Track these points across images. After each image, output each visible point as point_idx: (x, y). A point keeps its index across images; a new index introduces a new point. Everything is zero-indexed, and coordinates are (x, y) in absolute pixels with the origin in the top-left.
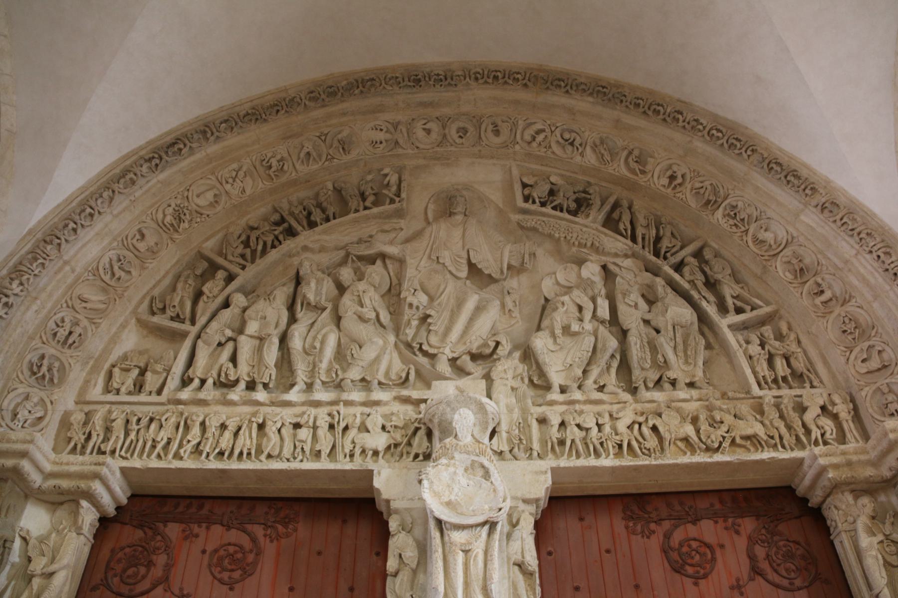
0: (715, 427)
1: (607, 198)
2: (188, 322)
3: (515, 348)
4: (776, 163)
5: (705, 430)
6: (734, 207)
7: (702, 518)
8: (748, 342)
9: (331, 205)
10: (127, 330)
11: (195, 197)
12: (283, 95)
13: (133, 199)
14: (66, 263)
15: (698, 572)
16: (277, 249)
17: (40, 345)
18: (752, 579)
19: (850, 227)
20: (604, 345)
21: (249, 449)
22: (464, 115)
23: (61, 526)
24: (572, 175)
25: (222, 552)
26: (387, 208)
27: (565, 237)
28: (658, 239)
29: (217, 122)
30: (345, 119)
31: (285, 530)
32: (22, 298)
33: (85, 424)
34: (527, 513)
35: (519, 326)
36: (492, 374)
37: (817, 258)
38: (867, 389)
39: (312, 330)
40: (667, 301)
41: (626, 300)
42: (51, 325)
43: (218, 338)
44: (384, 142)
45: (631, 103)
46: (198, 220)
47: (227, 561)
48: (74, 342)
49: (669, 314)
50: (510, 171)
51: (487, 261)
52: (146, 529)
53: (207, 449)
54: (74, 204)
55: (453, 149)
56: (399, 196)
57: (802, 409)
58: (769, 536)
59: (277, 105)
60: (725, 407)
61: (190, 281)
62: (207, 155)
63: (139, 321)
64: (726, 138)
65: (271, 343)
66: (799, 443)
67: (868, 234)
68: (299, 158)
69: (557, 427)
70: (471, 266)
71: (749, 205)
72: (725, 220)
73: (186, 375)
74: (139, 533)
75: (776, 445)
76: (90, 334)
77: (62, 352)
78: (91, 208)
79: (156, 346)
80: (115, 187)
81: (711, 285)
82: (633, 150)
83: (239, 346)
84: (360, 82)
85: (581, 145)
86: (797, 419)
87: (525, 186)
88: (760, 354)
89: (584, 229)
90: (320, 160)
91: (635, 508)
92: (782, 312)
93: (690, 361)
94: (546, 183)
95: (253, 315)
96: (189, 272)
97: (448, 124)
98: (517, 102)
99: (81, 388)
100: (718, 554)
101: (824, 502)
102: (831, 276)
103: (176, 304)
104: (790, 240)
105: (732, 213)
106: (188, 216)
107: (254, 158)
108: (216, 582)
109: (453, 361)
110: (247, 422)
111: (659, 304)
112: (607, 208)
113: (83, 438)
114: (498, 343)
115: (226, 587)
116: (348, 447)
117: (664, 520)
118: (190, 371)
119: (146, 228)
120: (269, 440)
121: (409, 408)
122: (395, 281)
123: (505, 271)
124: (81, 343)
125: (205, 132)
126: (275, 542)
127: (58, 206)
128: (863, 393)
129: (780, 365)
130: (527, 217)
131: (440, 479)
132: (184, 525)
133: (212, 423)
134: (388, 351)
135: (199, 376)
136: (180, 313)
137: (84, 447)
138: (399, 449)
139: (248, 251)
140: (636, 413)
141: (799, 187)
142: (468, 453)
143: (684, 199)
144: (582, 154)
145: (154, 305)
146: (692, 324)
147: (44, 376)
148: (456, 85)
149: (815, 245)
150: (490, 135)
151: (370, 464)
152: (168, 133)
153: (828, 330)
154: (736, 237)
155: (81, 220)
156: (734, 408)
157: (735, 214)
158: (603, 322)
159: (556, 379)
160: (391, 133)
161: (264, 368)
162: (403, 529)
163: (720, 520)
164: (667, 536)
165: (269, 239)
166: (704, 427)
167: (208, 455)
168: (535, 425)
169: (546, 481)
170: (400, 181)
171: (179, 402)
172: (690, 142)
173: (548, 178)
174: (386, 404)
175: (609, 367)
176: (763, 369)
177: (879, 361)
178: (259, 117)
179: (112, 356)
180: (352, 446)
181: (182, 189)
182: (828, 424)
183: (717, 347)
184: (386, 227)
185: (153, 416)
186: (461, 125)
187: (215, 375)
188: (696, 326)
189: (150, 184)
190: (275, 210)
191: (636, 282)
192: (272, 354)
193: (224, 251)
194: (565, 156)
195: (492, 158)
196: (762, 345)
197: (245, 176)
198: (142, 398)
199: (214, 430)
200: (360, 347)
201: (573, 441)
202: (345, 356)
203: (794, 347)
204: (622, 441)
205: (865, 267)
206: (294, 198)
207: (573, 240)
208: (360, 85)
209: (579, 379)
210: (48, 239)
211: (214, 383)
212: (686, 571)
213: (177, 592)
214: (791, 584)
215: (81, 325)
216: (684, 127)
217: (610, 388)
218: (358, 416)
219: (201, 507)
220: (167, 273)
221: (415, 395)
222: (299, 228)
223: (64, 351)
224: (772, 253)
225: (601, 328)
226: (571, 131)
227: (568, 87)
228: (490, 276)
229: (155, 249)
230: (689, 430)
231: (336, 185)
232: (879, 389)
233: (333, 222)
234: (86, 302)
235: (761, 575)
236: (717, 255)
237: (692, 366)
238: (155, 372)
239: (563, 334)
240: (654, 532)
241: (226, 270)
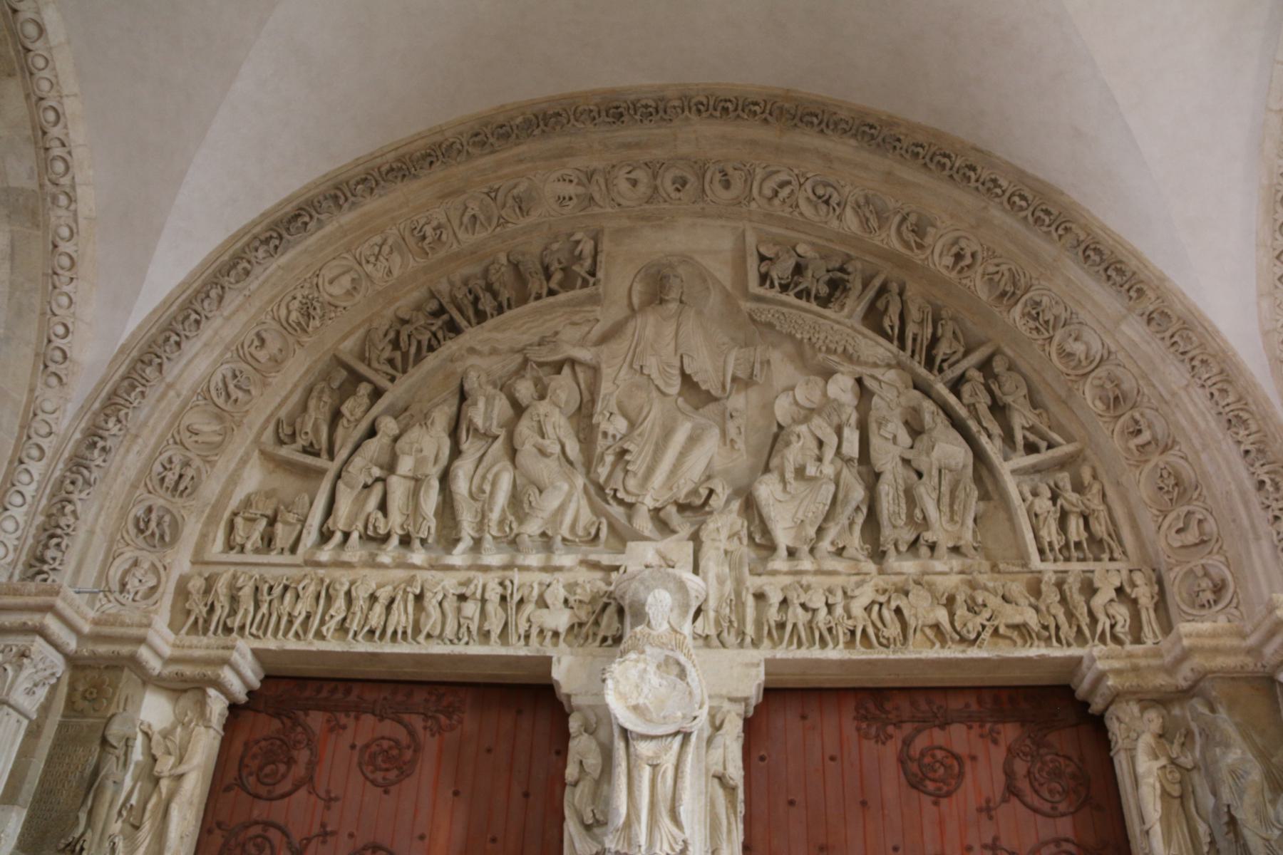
0: (975, 613)
1: (872, 277)
2: (325, 455)
3: (737, 493)
4: (1095, 249)
5: (962, 616)
6: (1038, 304)
7: (952, 722)
8: (1035, 494)
9: (505, 287)
10: (249, 466)
11: (326, 284)
12: (438, 138)
13: (247, 293)
14: (170, 386)
15: (940, 789)
16: (435, 353)
17: (146, 495)
18: (1005, 800)
19: (1181, 350)
20: (846, 496)
21: (405, 627)
22: (681, 159)
23: (187, 719)
24: (825, 243)
25: (374, 748)
26: (578, 293)
27: (810, 339)
28: (935, 340)
29: (352, 182)
30: (522, 167)
31: (448, 722)
32: (121, 438)
33: (207, 591)
34: (733, 714)
35: (742, 459)
36: (701, 534)
37: (1138, 384)
38: (1177, 569)
39: (481, 467)
40: (935, 434)
41: (882, 432)
42: (157, 468)
43: (363, 479)
44: (574, 197)
45: (907, 151)
46: (333, 315)
47: (380, 759)
48: (186, 488)
49: (935, 454)
50: (744, 237)
51: (704, 369)
52: (286, 720)
53: (354, 627)
54: (174, 308)
55: (666, 206)
57: (1090, 589)
58: (1034, 748)
59: (430, 155)
60: (990, 585)
61: (326, 398)
62: (341, 226)
63: (263, 453)
64: (1031, 209)
65: (429, 486)
66: (1080, 637)
67: (1203, 362)
68: (461, 224)
69: (777, 605)
70: (686, 378)
71: (1057, 303)
72: (1023, 322)
73: (325, 526)
74: (276, 724)
75: (1050, 638)
76: (204, 476)
77: (172, 502)
78: (197, 312)
79: (287, 485)
80: (225, 281)
81: (999, 409)
82: (908, 214)
83: (390, 490)
84: (540, 118)
85: (838, 204)
86: (1083, 603)
87: (762, 258)
88: (1049, 512)
89: (836, 327)
90: (490, 225)
91: (871, 705)
92: (1088, 452)
93: (956, 518)
94: (790, 257)
95: (407, 448)
96: (323, 384)
97: (661, 171)
98: (753, 143)
99: (197, 544)
100: (968, 766)
101: (1106, 708)
102: (1153, 412)
103: (309, 430)
104: (1106, 355)
105: (1034, 312)
106: (318, 310)
107: (402, 227)
108: (368, 784)
109: (656, 512)
110: (401, 593)
111: (925, 437)
112: (870, 294)
113: (205, 610)
114: (711, 492)
115: (380, 790)
116: (523, 627)
117: (905, 722)
118: (330, 521)
119: (266, 331)
120: (428, 616)
121: (598, 575)
122: (586, 396)
123: (728, 386)
124: (195, 489)
125: (336, 197)
126: (437, 736)
127: (155, 311)
128: (1172, 575)
129: (1075, 528)
130: (764, 306)
131: (627, 678)
132: (329, 714)
133: (359, 593)
134: (575, 498)
135: (341, 527)
136: (314, 442)
137: (207, 622)
138: (584, 630)
139: (398, 355)
140: (877, 591)
141: (1121, 286)
142: (662, 646)
143: (973, 288)
144: (839, 218)
145: (280, 430)
146: (965, 466)
147: (153, 534)
148: (671, 120)
149: (1138, 366)
150: (718, 187)
151: (549, 650)
152: (288, 200)
153: (1141, 485)
154: (1036, 346)
155: (184, 330)
156: (1003, 586)
157: (1038, 314)
158: (848, 461)
159: (783, 538)
160: (584, 185)
161: (421, 519)
162: (586, 731)
163: (976, 725)
164: (907, 743)
165: (425, 337)
166: (961, 611)
167: (356, 634)
168: (750, 601)
169: (757, 676)
170: (596, 253)
171: (319, 564)
172: (985, 208)
173: (794, 249)
174: (570, 569)
175: (851, 524)
176: (1050, 532)
177: (1197, 533)
178: (407, 173)
179: (232, 502)
180: (527, 625)
181: (309, 275)
182: (1122, 613)
183: (996, 497)
184: (576, 318)
185: (288, 583)
186: (678, 173)
187: (361, 527)
188: (970, 470)
189: (268, 272)
190: (432, 295)
191: (899, 404)
192: (431, 500)
193: (367, 355)
194: (817, 219)
195: (720, 217)
196: (1054, 499)
197: (391, 252)
198: (273, 557)
199: (361, 602)
200: (541, 492)
201: (795, 625)
202: (521, 502)
203: (1096, 503)
204: (855, 627)
205: (1195, 405)
206: (457, 278)
207: (820, 342)
208: (541, 123)
209: (811, 540)
210: (146, 358)
211: (360, 537)
212: (925, 786)
213: (322, 794)
214: (1053, 808)
215: (194, 466)
216: (977, 189)
217: (850, 552)
218: (536, 586)
219: (348, 692)
220: (295, 386)
221: (606, 559)
223: (174, 500)
224: (1081, 372)
225: (845, 472)
226: (826, 185)
227: (823, 126)
228: (708, 392)
229: (279, 357)
230: (942, 615)
231: (511, 258)
232: (1191, 571)
233: (508, 314)
234: (197, 434)
235: (1017, 795)
236: (1011, 367)
237: (958, 526)
238: (286, 523)
239: (796, 478)
240: (891, 737)
241: (369, 381)
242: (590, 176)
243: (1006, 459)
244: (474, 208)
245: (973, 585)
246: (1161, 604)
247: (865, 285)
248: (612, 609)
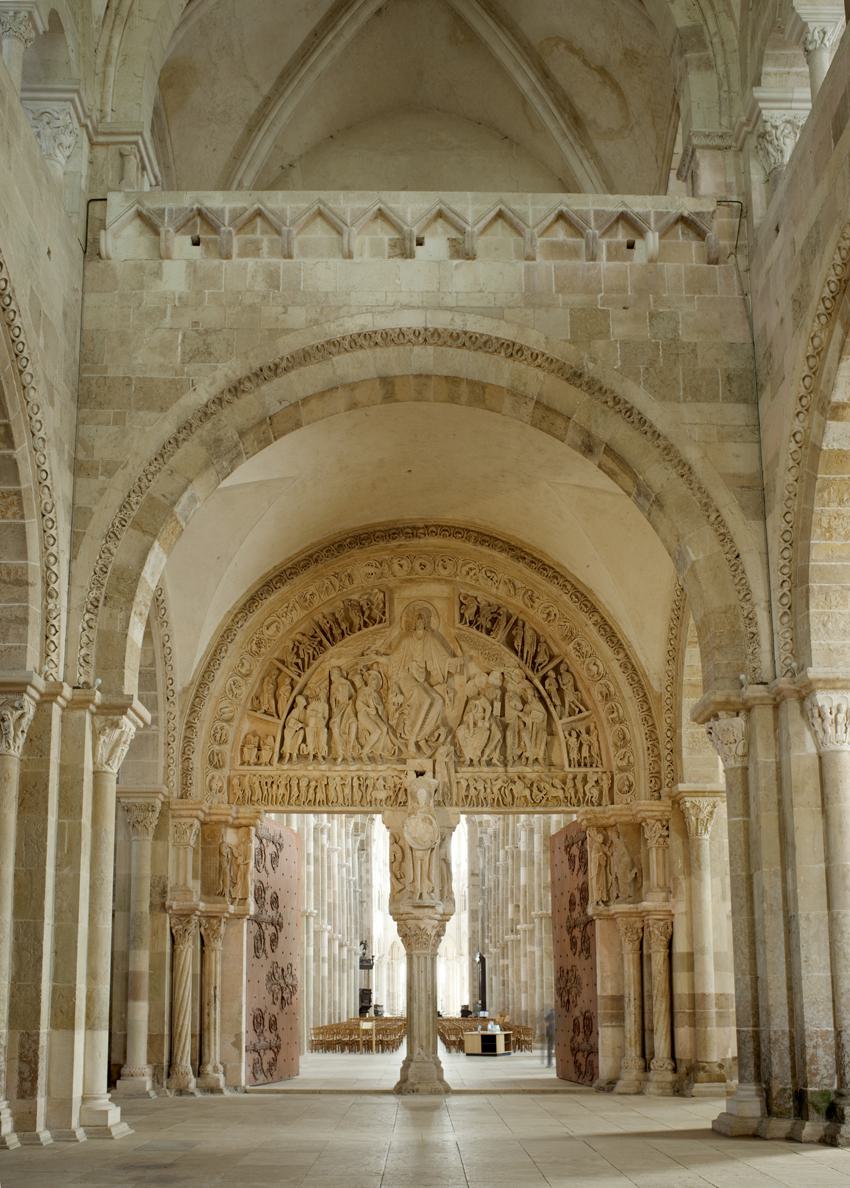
8: (570, 735)
26: (376, 626)
35: (452, 714)
56: (384, 613)
57: (585, 780)
70: (428, 674)
81: (560, 690)
87: (462, 604)
121: (396, 773)
139: (300, 661)
165: (311, 652)
168: (454, 785)
175: (496, 747)
176: (574, 755)
182: (595, 792)
196: (578, 736)
222: (328, 644)
230: (527, 792)
233: (348, 638)
236: (568, 671)
243: (560, 718)
245: (540, 776)
246: (611, 788)
247: (507, 622)
248: (403, 790)
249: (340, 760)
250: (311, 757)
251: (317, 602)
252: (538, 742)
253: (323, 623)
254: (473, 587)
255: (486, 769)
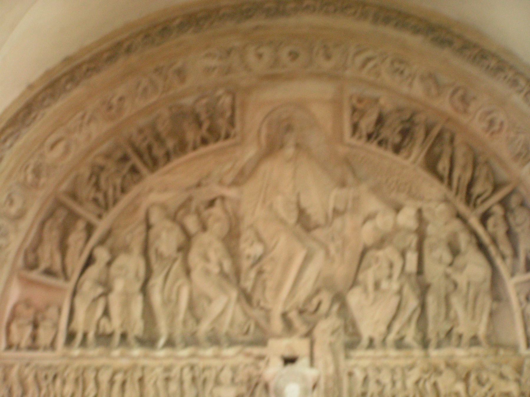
109: (284, 315)
139: (100, 196)
158: (409, 275)
165: (118, 181)
175: (410, 319)
233: (176, 162)
242: (229, 52)
243: (513, 275)
244: (144, 82)
249: (162, 341)
250: (117, 338)
251: (129, 110)
252: (478, 310)
253: (138, 139)
254: (373, 85)
255: (393, 353)
